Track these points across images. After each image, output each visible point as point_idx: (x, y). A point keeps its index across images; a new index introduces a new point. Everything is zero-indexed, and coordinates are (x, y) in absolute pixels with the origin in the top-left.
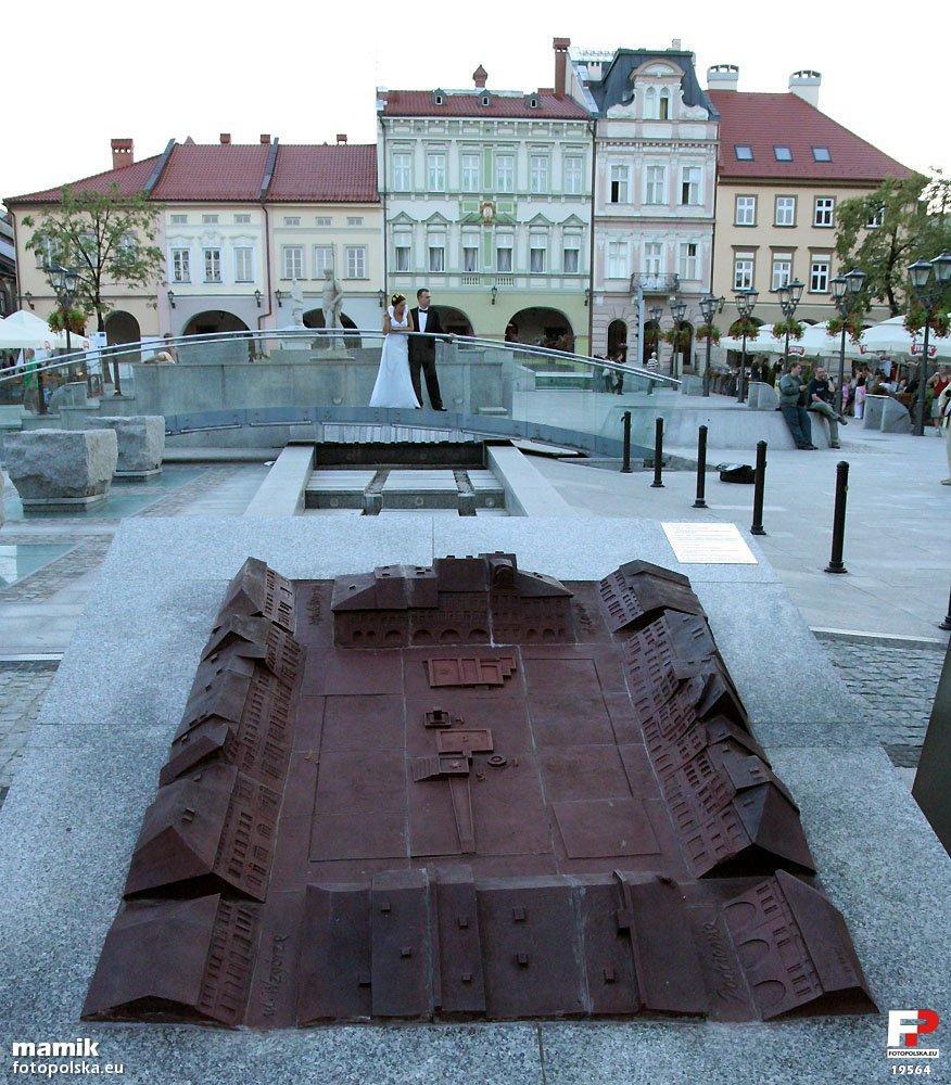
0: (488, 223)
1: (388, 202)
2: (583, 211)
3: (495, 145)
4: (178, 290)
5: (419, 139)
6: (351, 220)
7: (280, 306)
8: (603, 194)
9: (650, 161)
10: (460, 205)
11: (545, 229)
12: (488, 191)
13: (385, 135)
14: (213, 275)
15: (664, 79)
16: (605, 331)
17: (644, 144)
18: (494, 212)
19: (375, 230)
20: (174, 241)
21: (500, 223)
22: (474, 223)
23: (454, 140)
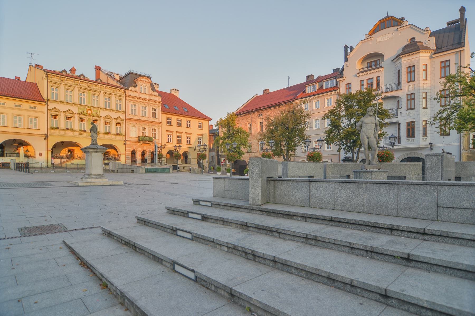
1: (49, 103)
6: (31, 107)
10: (79, 108)
13: (48, 80)
15: (146, 83)
16: (130, 153)
19: (43, 112)
21: (94, 116)
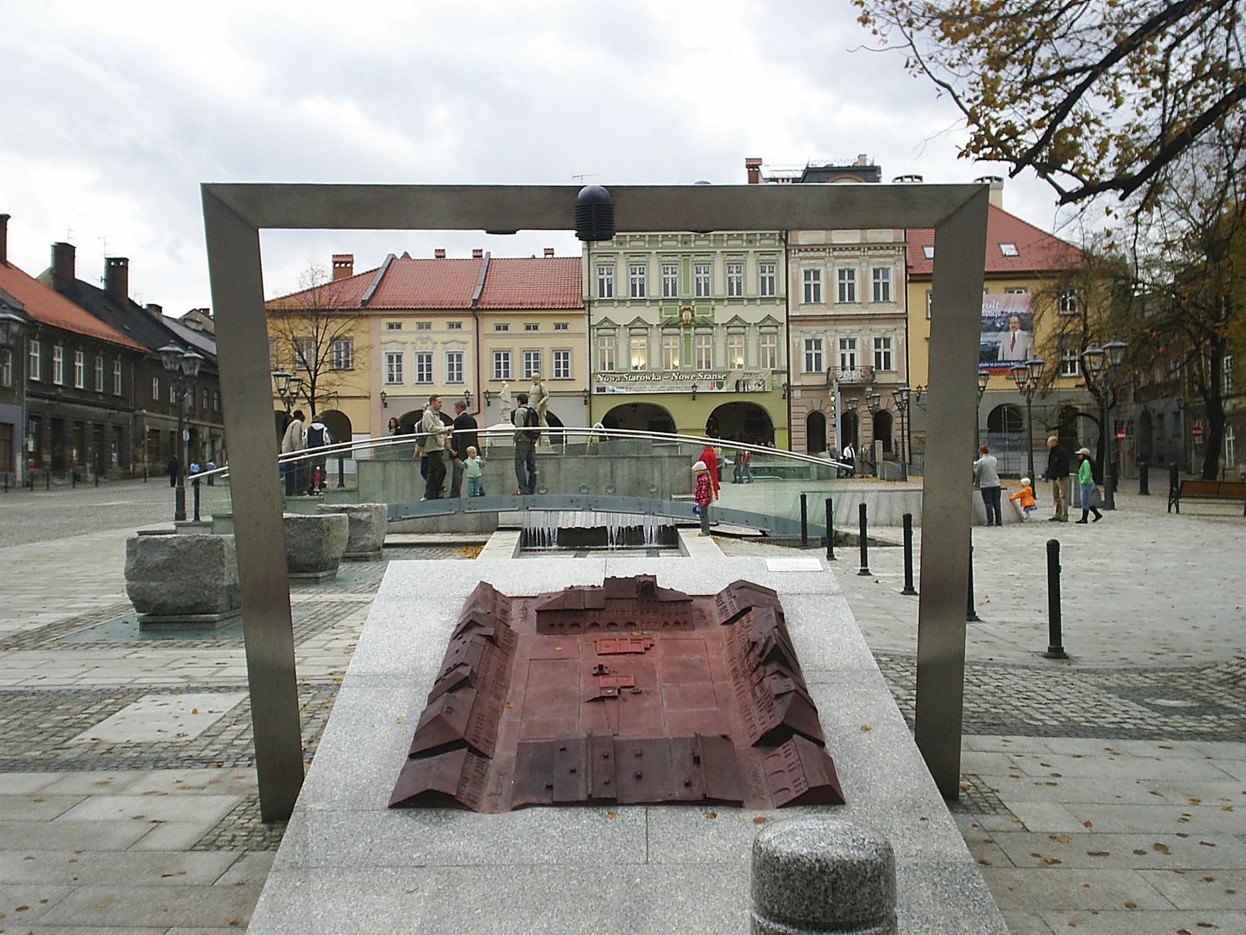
0: (687, 326)
2: (779, 313)
3: (692, 255)
4: (390, 391)
5: (621, 252)
6: (557, 327)
7: (489, 405)
8: (796, 296)
9: (842, 264)
10: (661, 310)
11: (742, 330)
12: (686, 297)
13: (589, 251)
14: (425, 374)
16: (804, 422)
17: (834, 250)
18: (693, 315)
19: (581, 335)
20: (388, 346)
22: (673, 326)
23: (654, 252)
